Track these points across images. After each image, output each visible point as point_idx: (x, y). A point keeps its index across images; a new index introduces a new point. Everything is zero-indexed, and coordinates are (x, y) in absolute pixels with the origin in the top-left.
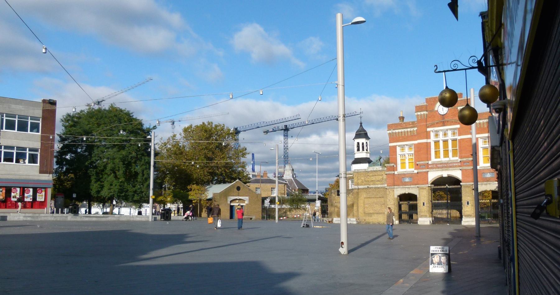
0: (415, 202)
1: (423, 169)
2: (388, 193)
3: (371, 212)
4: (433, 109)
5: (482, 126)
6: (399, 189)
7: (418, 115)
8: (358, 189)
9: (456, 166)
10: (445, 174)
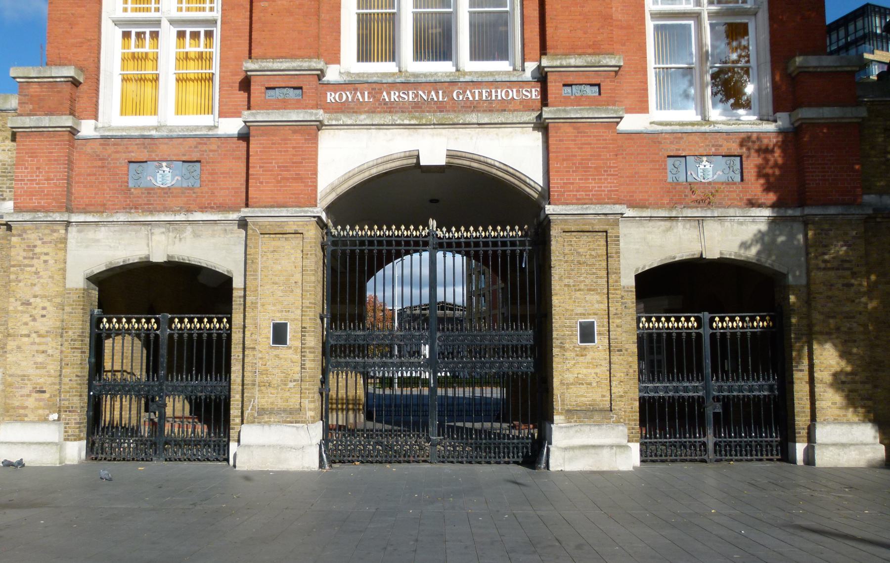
0: (211, 324)
1: (284, 105)
2: (18, 253)
6: (102, 233)
9: (504, 106)
10: (434, 148)
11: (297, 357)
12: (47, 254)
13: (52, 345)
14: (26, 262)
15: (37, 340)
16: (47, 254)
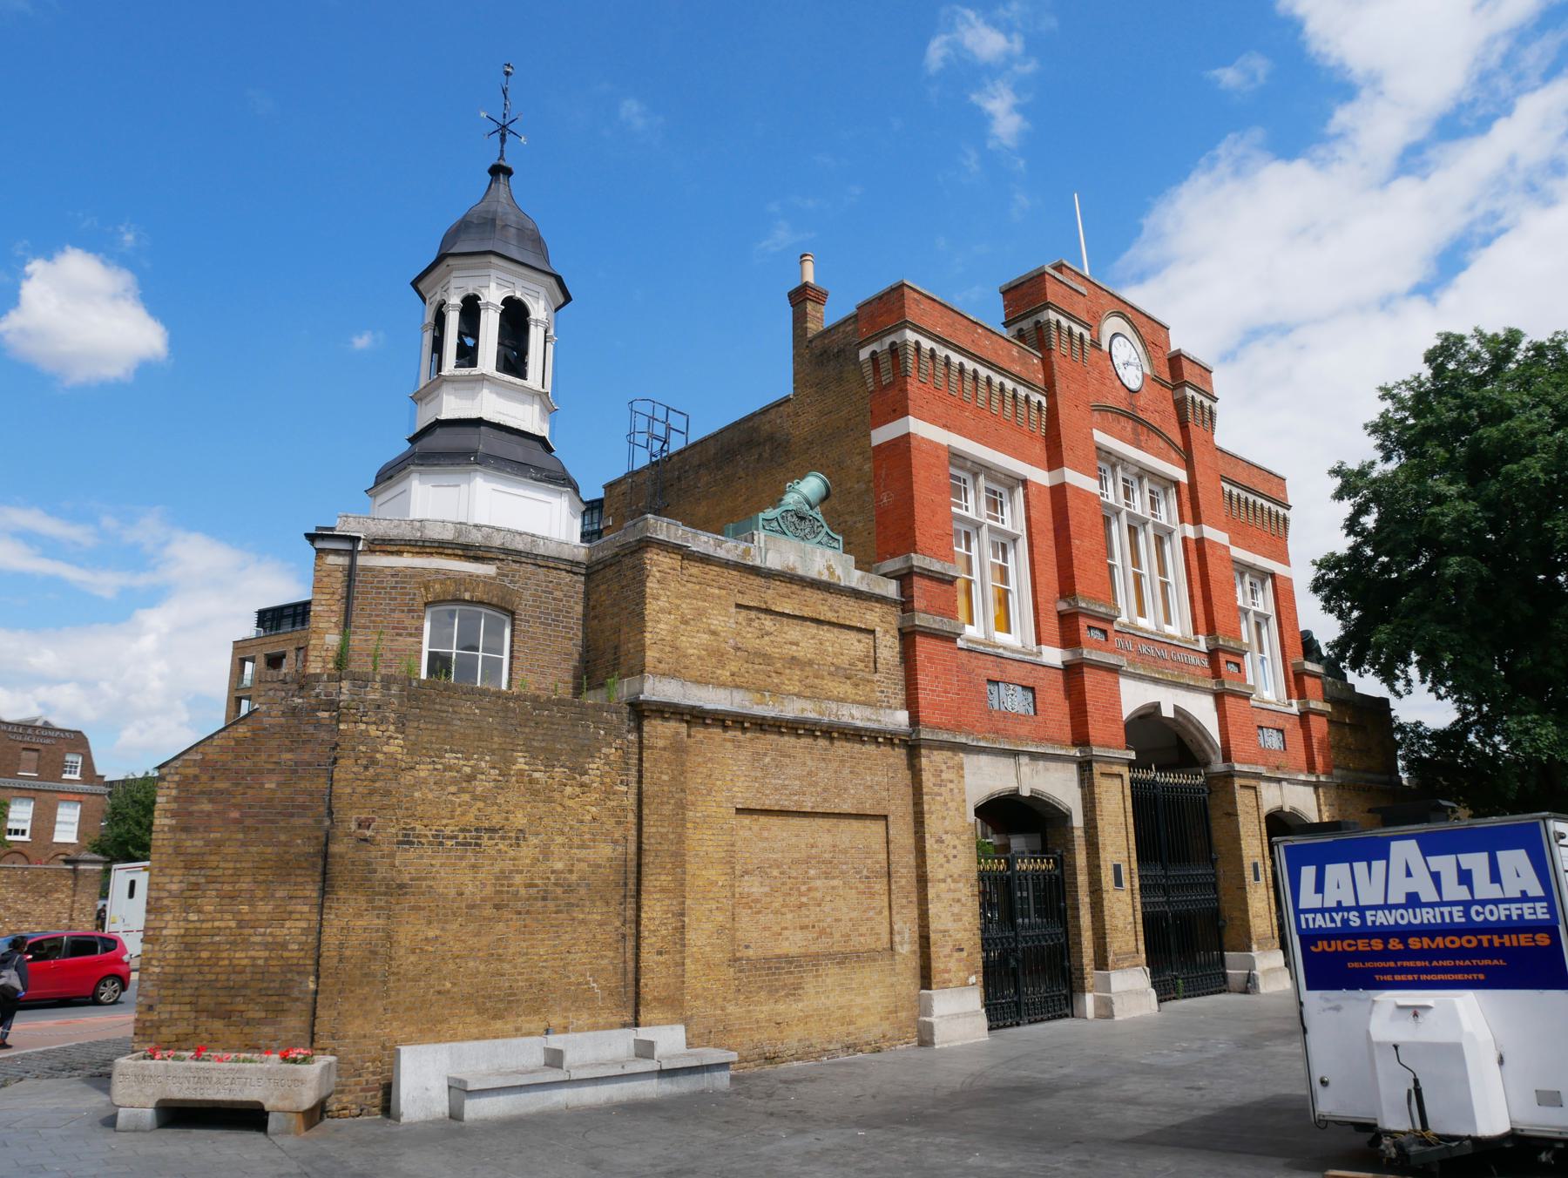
3: (793, 943)
14: (936, 789)
15: (953, 886)
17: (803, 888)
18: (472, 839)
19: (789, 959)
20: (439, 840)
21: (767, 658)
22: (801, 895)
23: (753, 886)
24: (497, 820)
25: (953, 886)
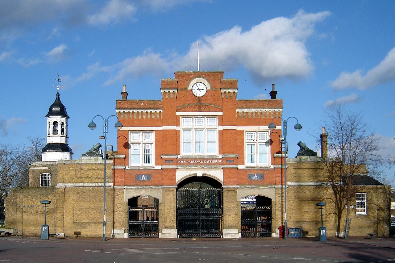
3: (85, 221)
4: (186, 89)
5: (250, 117)
7: (165, 93)
8: (65, 188)
11: (173, 216)
12: (120, 195)
13: (122, 213)
15: (119, 212)
16: (120, 195)
17: (88, 213)
18: (32, 206)
19: (84, 223)
20: (28, 207)
21: (82, 177)
22: (87, 213)
23: (78, 212)
24: (36, 204)
25: (119, 212)
